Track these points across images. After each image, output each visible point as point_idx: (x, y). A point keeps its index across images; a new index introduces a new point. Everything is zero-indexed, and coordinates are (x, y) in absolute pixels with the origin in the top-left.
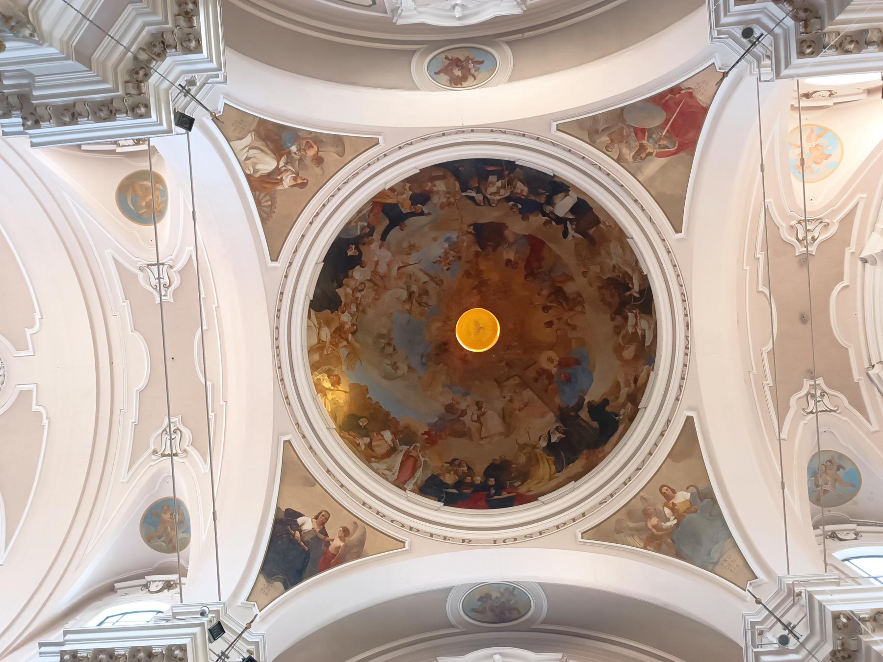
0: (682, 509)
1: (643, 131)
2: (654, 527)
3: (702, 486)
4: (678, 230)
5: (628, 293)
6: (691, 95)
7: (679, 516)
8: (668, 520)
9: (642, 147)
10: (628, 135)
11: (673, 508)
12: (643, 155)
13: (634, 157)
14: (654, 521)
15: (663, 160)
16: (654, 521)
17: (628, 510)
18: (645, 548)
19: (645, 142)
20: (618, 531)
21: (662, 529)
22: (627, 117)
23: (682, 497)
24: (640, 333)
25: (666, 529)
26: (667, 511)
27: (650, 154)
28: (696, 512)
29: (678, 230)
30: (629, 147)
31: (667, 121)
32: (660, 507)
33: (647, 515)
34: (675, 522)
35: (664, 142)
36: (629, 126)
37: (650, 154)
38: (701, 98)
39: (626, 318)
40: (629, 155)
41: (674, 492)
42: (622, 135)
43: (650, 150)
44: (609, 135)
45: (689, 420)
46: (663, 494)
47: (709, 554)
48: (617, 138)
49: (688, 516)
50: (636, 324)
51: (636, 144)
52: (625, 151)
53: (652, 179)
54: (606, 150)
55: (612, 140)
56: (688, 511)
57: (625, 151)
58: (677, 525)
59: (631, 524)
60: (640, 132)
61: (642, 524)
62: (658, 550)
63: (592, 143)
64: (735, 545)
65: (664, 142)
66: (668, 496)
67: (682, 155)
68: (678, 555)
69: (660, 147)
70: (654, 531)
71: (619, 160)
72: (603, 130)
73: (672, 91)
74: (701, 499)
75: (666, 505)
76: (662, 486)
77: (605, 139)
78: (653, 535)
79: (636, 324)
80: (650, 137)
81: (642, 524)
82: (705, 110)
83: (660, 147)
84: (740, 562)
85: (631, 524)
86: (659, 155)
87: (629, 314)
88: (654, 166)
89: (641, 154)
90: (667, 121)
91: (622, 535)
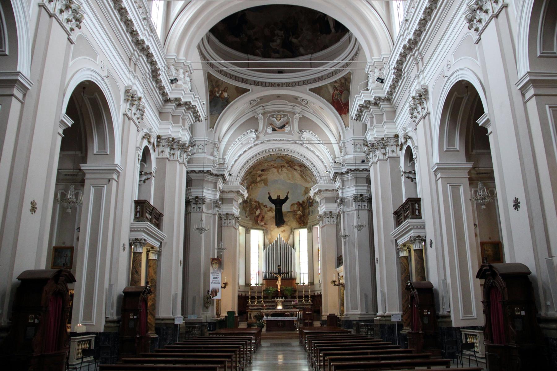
0: (222, 96)
1: (342, 93)
2: (215, 91)
3: (230, 100)
4: (310, 90)
5: (291, 34)
6: (345, 114)
7: (220, 96)
8: (218, 94)
9: (337, 90)
10: (342, 88)
11: (222, 93)
12: (335, 89)
13: (335, 86)
14: (217, 89)
15: (332, 94)
16: (217, 89)
17: (218, 80)
18: (209, 91)
19: (338, 91)
20: (211, 81)
21: (215, 93)
22: (347, 92)
23: (225, 95)
24: (275, 38)
25: (215, 94)
26: (220, 92)
27: (335, 91)
28: (222, 101)
29: (310, 90)
30: (338, 86)
31: (342, 102)
32: (221, 89)
33: (218, 86)
34: (218, 96)
35: (336, 97)
36: (344, 90)
37: (335, 91)
38: (343, 116)
39: (281, 30)
40: (337, 85)
41: (226, 92)
42: (342, 86)
43: (336, 92)
44: (344, 83)
45: (249, 90)
46: (225, 88)
47: (213, 111)
48: (342, 85)
49: (220, 99)
50: (278, 36)
51: (339, 88)
52: (338, 85)
53: (327, 88)
54: (340, 80)
55: (342, 83)
56: (222, 98)
57: (338, 85)
58: (218, 97)
59: (214, 84)
60: (341, 92)
61: (215, 86)
62: (210, 96)
63: (343, 77)
64: (218, 117)
65: (336, 97)
66: (225, 90)
67: (331, 100)
68: (210, 102)
69: (335, 95)
70: (214, 91)
71: (335, 82)
72: (346, 83)
73: (348, 109)
74: (226, 101)
75: (222, 90)
76: (227, 87)
77: (343, 81)
78: (213, 91)
79: (278, 36)
80: (339, 94)
81: (215, 86)
82: (340, 114)
83: (335, 95)
84: (214, 122)
85: (214, 84)
86: (333, 93)
87: (282, 32)
88: (331, 90)
89: (335, 89)
90: (342, 102)
91: (210, 83)
